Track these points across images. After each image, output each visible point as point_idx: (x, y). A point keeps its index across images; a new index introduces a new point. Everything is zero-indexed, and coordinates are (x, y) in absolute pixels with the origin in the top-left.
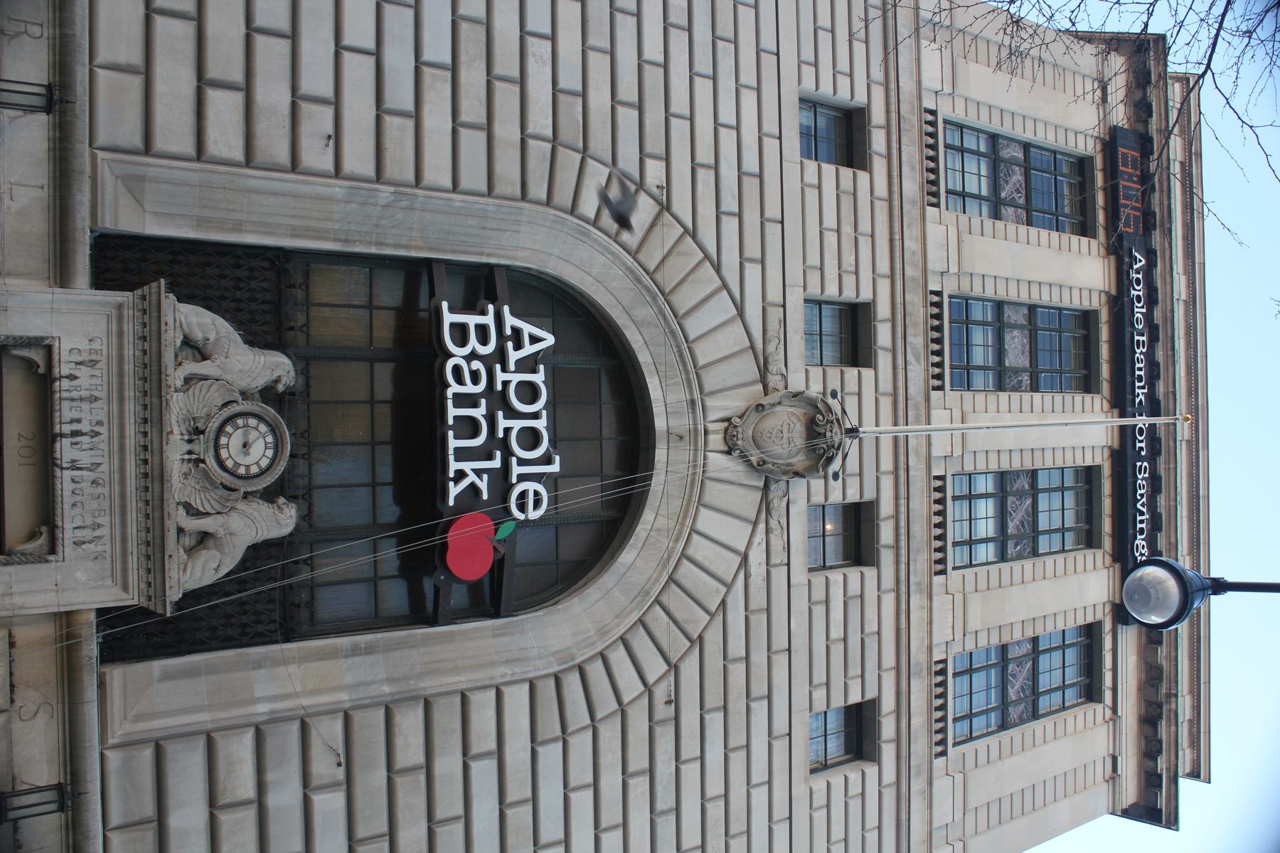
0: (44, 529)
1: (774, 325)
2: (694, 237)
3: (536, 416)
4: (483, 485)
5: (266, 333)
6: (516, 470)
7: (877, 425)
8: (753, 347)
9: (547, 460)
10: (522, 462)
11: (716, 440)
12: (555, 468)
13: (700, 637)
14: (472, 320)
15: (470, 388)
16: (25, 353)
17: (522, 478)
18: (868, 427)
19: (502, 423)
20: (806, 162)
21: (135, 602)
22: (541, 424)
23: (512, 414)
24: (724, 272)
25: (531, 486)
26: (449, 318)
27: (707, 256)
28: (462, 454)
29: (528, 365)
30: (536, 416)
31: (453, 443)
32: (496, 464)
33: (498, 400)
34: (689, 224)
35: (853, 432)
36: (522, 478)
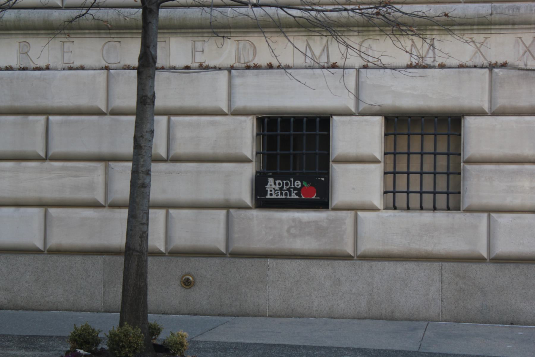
3: (283, 183)
4: (295, 192)
6: (292, 186)
9: (291, 181)
10: (291, 185)
12: (292, 179)
14: (269, 192)
15: (279, 194)
17: (294, 185)
19: (285, 189)
22: (285, 182)
23: (283, 187)
25: (296, 184)
26: (268, 196)
28: (290, 195)
29: (275, 184)
30: (283, 183)
31: (288, 197)
32: (292, 190)
33: (281, 189)
36: (294, 185)
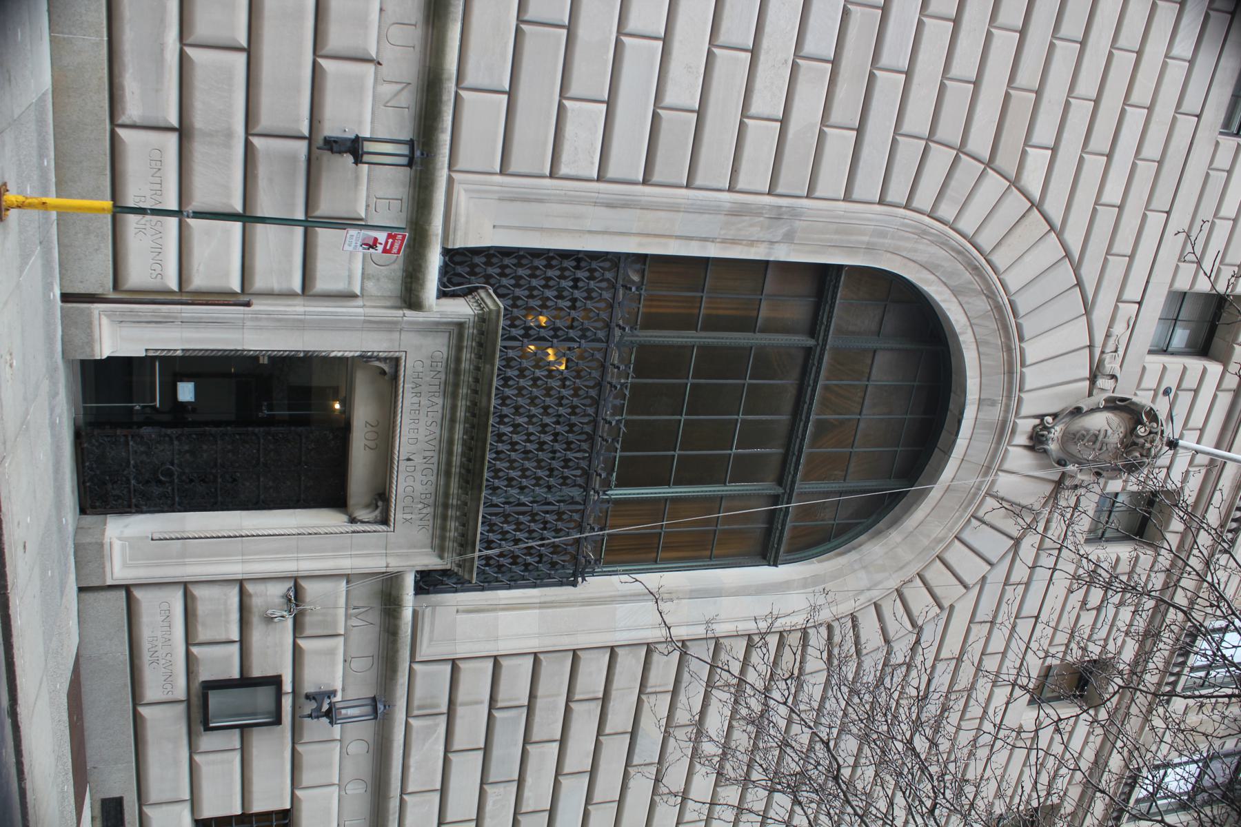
0: (380, 503)
1: (1120, 329)
2: (1059, 236)
5: (596, 329)
7: (1198, 443)
8: (1091, 347)
11: (1021, 439)
13: (952, 607)
16: (377, 364)
18: (1188, 441)
20: (1222, 139)
21: (448, 567)
24: (1084, 271)
27: (1068, 255)
34: (1058, 223)
35: (1173, 444)
